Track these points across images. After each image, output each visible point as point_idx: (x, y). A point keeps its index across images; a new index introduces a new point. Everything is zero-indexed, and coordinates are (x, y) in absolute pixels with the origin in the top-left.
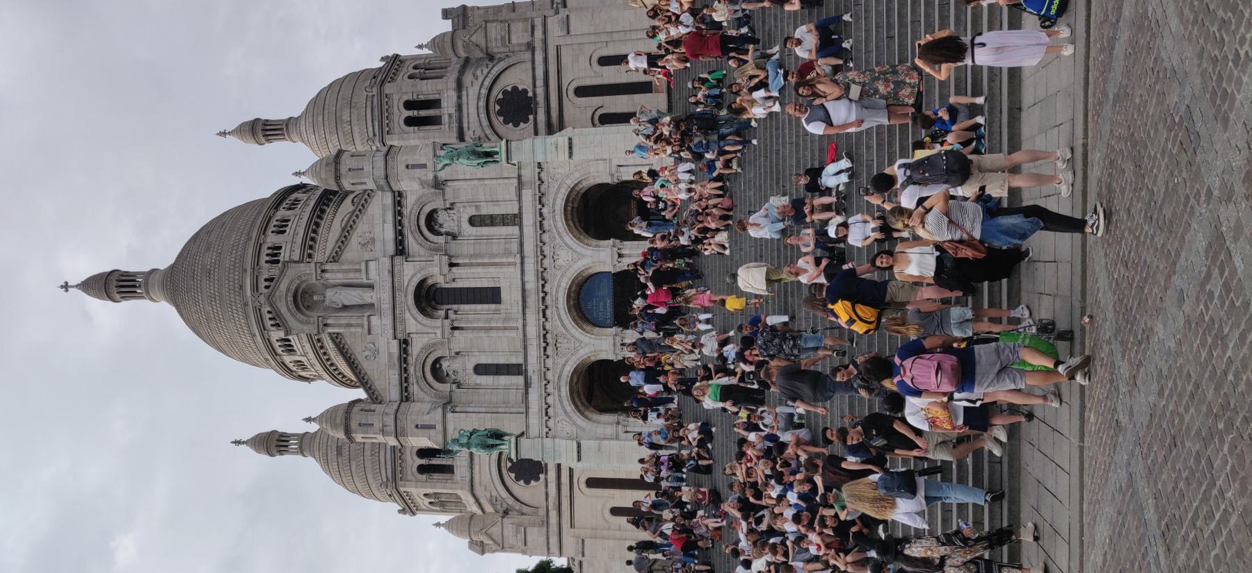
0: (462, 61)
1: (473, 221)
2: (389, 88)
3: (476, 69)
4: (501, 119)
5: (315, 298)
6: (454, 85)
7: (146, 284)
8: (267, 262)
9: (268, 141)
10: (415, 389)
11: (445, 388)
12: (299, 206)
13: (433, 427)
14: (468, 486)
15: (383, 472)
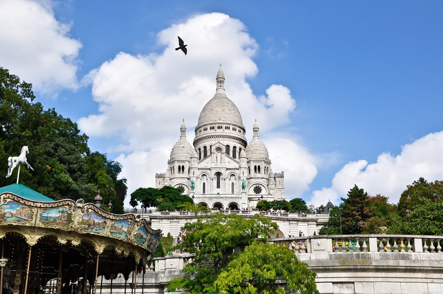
0: (268, 178)
1: (233, 183)
2: (263, 162)
3: (266, 182)
4: (255, 187)
5: (219, 151)
6: (262, 177)
7: (221, 89)
8: (226, 126)
9: (254, 131)
10: (201, 171)
11: (201, 177)
12: (239, 133)
13: (194, 175)
14: (175, 177)
15: (179, 158)
